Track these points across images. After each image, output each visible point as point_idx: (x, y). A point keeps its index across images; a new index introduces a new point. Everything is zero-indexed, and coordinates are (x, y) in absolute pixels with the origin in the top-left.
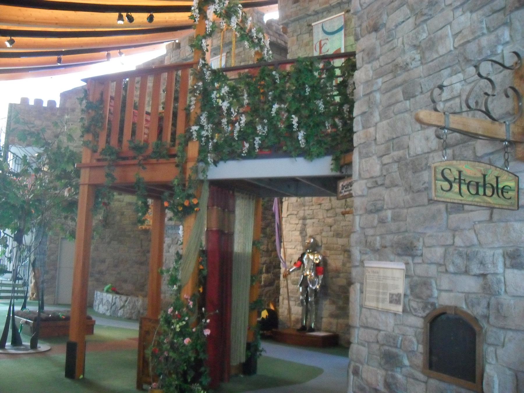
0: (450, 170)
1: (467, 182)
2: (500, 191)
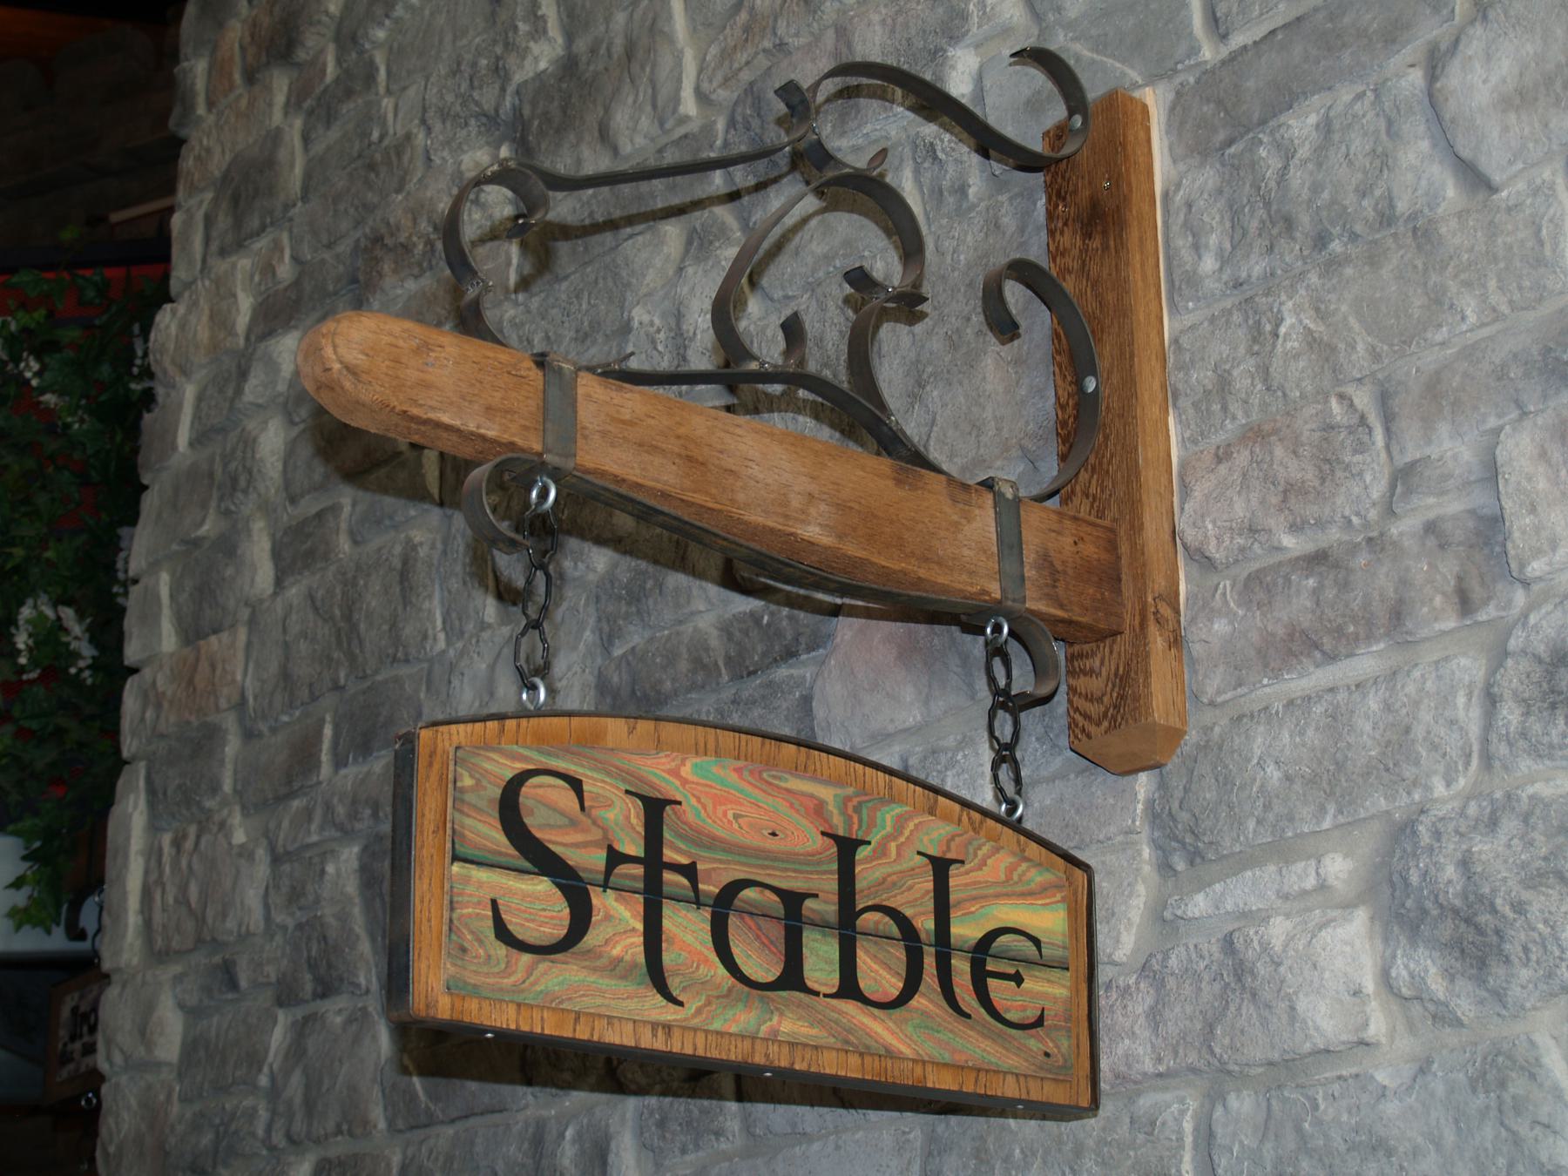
0: (576, 785)
1: (710, 888)
2: (961, 967)
